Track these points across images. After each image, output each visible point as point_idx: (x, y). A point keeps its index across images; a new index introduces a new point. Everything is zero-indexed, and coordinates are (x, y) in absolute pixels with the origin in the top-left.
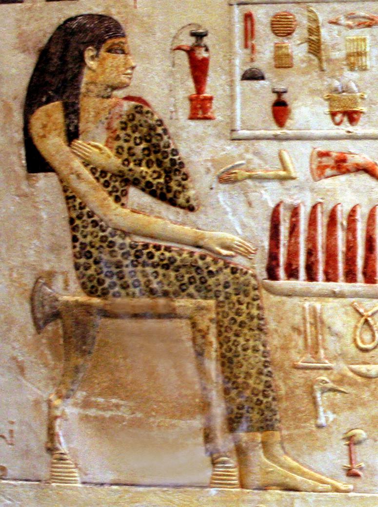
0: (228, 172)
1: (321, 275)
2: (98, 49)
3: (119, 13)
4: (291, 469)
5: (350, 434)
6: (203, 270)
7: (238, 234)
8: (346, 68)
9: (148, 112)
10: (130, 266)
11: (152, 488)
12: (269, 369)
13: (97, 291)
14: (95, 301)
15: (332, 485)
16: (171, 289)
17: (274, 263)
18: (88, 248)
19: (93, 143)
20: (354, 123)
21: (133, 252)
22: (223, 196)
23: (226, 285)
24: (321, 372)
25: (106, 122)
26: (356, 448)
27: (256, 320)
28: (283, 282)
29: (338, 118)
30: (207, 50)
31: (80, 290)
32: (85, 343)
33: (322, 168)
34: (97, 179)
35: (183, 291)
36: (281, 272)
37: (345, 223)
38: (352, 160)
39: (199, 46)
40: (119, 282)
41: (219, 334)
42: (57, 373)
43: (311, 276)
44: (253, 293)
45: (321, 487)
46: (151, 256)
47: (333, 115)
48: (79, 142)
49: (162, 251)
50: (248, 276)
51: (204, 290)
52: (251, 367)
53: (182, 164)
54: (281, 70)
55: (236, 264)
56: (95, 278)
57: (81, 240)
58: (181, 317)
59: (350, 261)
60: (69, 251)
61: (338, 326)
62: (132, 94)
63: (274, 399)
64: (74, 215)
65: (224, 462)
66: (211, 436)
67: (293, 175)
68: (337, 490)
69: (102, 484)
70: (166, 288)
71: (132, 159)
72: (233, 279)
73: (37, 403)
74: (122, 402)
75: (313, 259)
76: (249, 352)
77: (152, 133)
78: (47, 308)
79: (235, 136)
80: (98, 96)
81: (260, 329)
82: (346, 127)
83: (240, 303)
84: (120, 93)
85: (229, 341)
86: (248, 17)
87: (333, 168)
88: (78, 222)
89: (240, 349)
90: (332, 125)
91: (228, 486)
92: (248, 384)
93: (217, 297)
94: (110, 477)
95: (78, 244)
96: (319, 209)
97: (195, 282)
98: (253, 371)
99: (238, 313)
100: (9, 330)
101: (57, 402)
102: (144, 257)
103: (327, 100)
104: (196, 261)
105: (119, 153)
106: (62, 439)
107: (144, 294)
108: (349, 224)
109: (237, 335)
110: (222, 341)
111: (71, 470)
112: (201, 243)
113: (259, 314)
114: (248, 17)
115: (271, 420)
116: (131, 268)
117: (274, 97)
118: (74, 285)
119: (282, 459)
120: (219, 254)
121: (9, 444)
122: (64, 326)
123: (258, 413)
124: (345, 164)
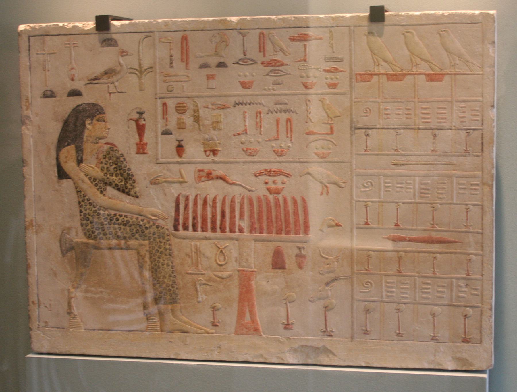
0: (154, 179)
1: (199, 229)
2: (92, 120)
3: (102, 102)
4: (185, 322)
5: (213, 306)
7: (160, 209)
8: (212, 129)
9: (116, 150)
11: (119, 332)
12: (175, 274)
13: (91, 236)
14: (91, 241)
15: (205, 330)
16: (127, 236)
17: (177, 223)
18: (87, 216)
19: (89, 165)
21: (109, 218)
22: (152, 191)
23: (154, 234)
24: (200, 275)
25: (96, 155)
26: (217, 313)
27: (168, 251)
28: (181, 232)
29: (208, 153)
30: (145, 120)
31: (83, 236)
32: (86, 262)
33: (200, 177)
34: (92, 182)
35: (133, 236)
36: (180, 227)
37: (211, 204)
39: (140, 118)
40: (102, 232)
41: (151, 257)
43: (195, 230)
44: (167, 238)
45: (199, 331)
46: (117, 220)
47: (205, 151)
48: (83, 165)
49: (123, 217)
50: (164, 229)
51: (143, 236)
53: (132, 175)
54: (180, 130)
57: (84, 212)
58: (132, 249)
59: (214, 222)
60: (78, 217)
61: (208, 254)
62: (109, 142)
63: (177, 289)
64: (81, 200)
65: (153, 319)
67: (186, 180)
68: (207, 333)
69: (94, 330)
70: (125, 235)
71: (108, 173)
73: (63, 290)
75: (195, 221)
76: (165, 266)
77: (118, 160)
78: (68, 245)
79: (158, 162)
80: (92, 142)
81: (170, 255)
82: (211, 158)
83: (161, 242)
84: (103, 141)
86: (164, 104)
87: (205, 177)
88: (82, 203)
89: (160, 264)
92: (164, 282)
93: (150, 239)
94: (98, 326)
95: (82, 214)
96: (199, 196)
98: (167, 275)
99: (160, 247)
101: (72, 290)
102: (114, 220)
104: (139, 222)
105: (102, 170)
106: (75, 308)
109: (159, 258)
112: (142, 213)
114: (164, 104)
116: (108, 226)
117: (177, 143)
118: (81, 234)
120: (151, 219)
122: (76, 253)
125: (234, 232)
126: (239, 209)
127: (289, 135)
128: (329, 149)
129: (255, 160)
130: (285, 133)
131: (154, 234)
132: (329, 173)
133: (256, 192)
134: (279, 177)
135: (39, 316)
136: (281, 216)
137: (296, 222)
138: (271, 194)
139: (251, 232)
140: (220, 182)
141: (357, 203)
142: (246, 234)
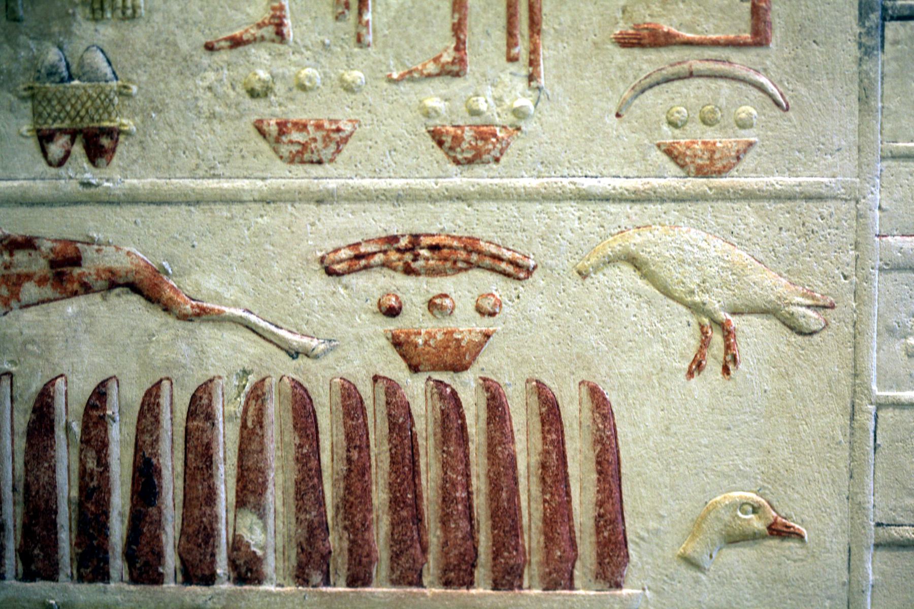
20: (102, 161)
29: (56, 149)
37: (77, 428)
38: (93, 263)
47: (45, 138)
59: (91, 522)
87: (42, 282)
90: (42, 166)
103: (23, 99)
108: (85, 429)
124: (77, 271)
125: (209, 579)
126: (233, 459)
127: (522, 49)
128: (743, 125)
129: (332, 184)
130: (499, 36)
132: (739, 255)
133: (330, 359)
134: (463, 276)
136: (467, 486)
137: (557, 515)
138: (414, 369)
139: (301, 577)
140: (135, 302)
141: (887, 415)
142: (276, 585)
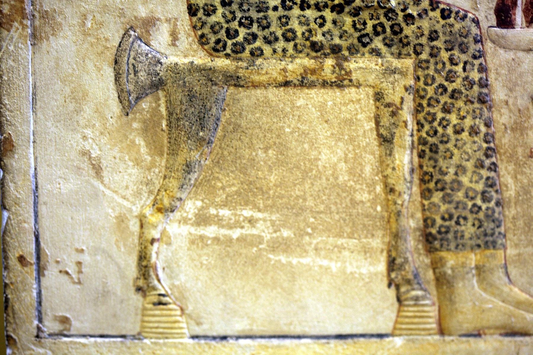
6: (397, 14)
10: (280, 9)
12: (494, 160)
13: (225, 47)
14: (222, 63)
16: (344, 44)
23: (433, 36)
27: (476, 88)
35: (365, 45)
41: (418, 109)
42: (155, 177)
44: (473, 48)
51: (397, 41)
52: (466, 157)
55: (448, 5)
56: (222, 27)
58: (358, 86)
63: (498, 204)
65: (417, 299)
66: (399, 261)
69: (224, 338)
70: (337, 41)
72: (443, 26)
73: (121, 220)
74: (259, 215)
76: (465, 135)
78: (142, 76)
81: (482, 100)
85: (434, 120)
89: (450, 130)
91: (423, 333)
92: (459, 183)
93: (417, 54)
97: (384, 31)
99: (450, 77)
100: (78, 111)
107: (301, 52)
109: (446, 110)
110: (423, 121)
111: (174, 319)
113: (481, 78)
115: (492, 235)
116: (281, 12)
118: (187, 39)
119: (506, 289)
121: (74, 283)
122: (169, 102)
123: (474, 225)
131: (433, 36)
135: (40, 303)
